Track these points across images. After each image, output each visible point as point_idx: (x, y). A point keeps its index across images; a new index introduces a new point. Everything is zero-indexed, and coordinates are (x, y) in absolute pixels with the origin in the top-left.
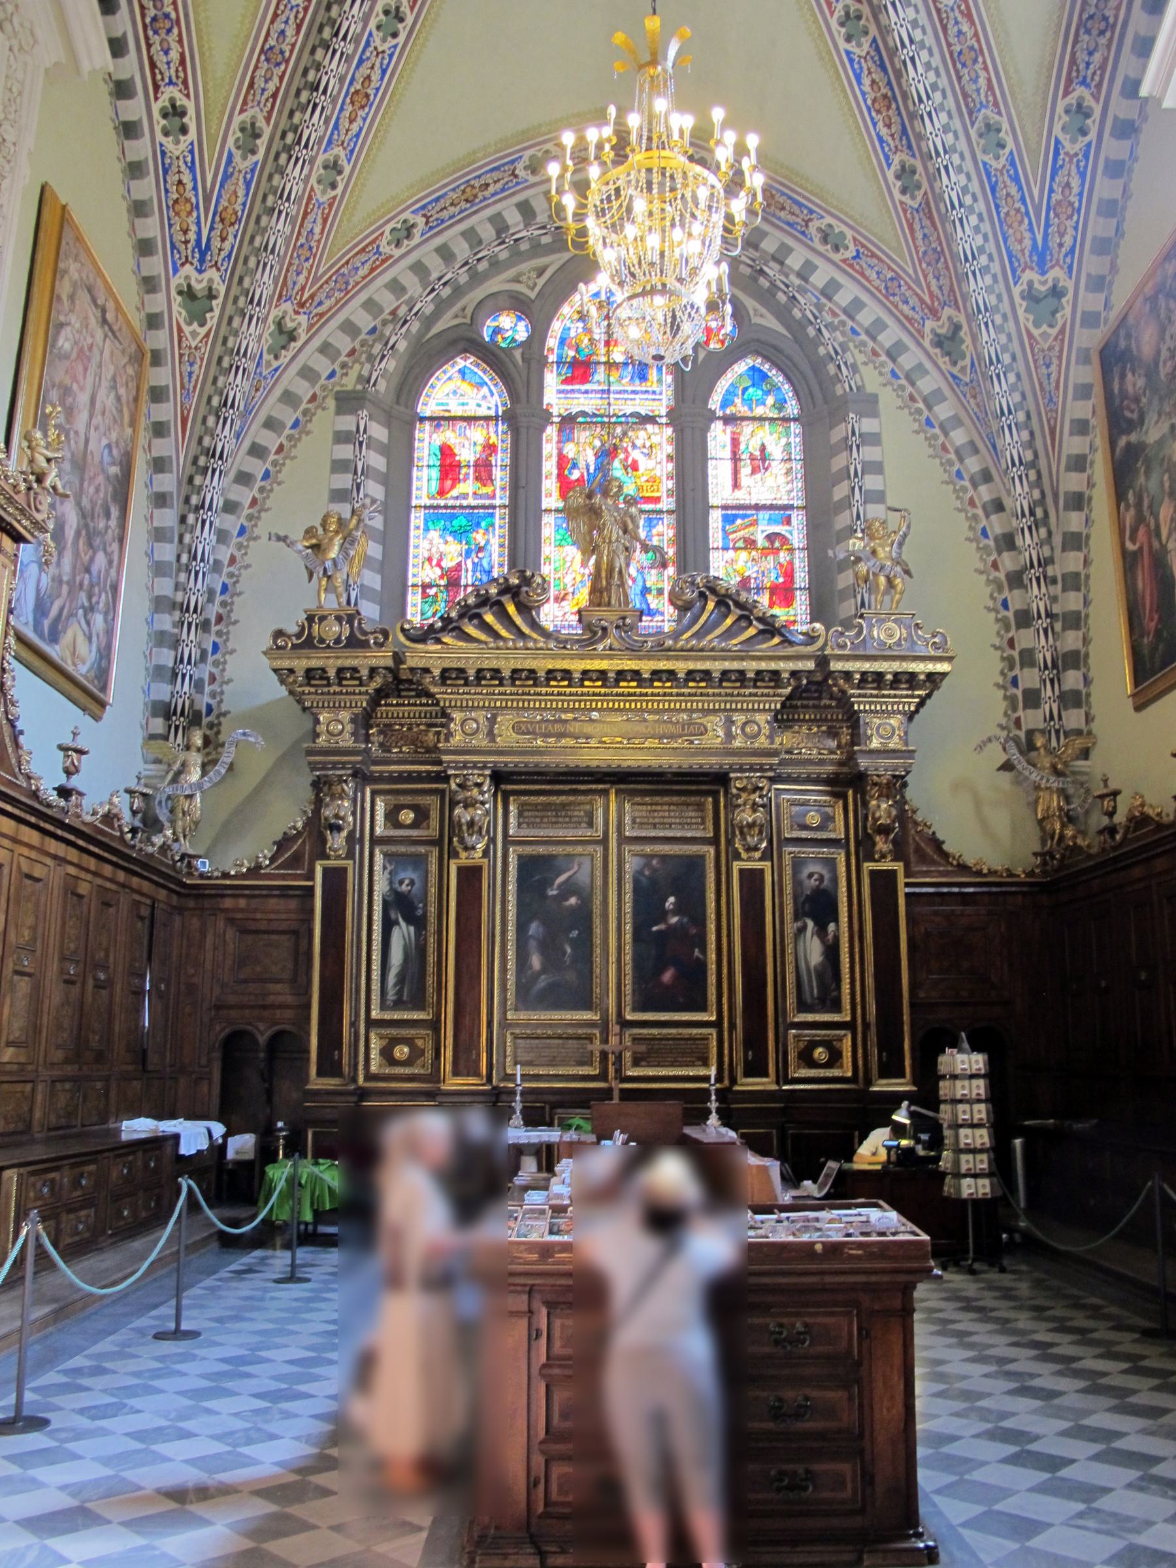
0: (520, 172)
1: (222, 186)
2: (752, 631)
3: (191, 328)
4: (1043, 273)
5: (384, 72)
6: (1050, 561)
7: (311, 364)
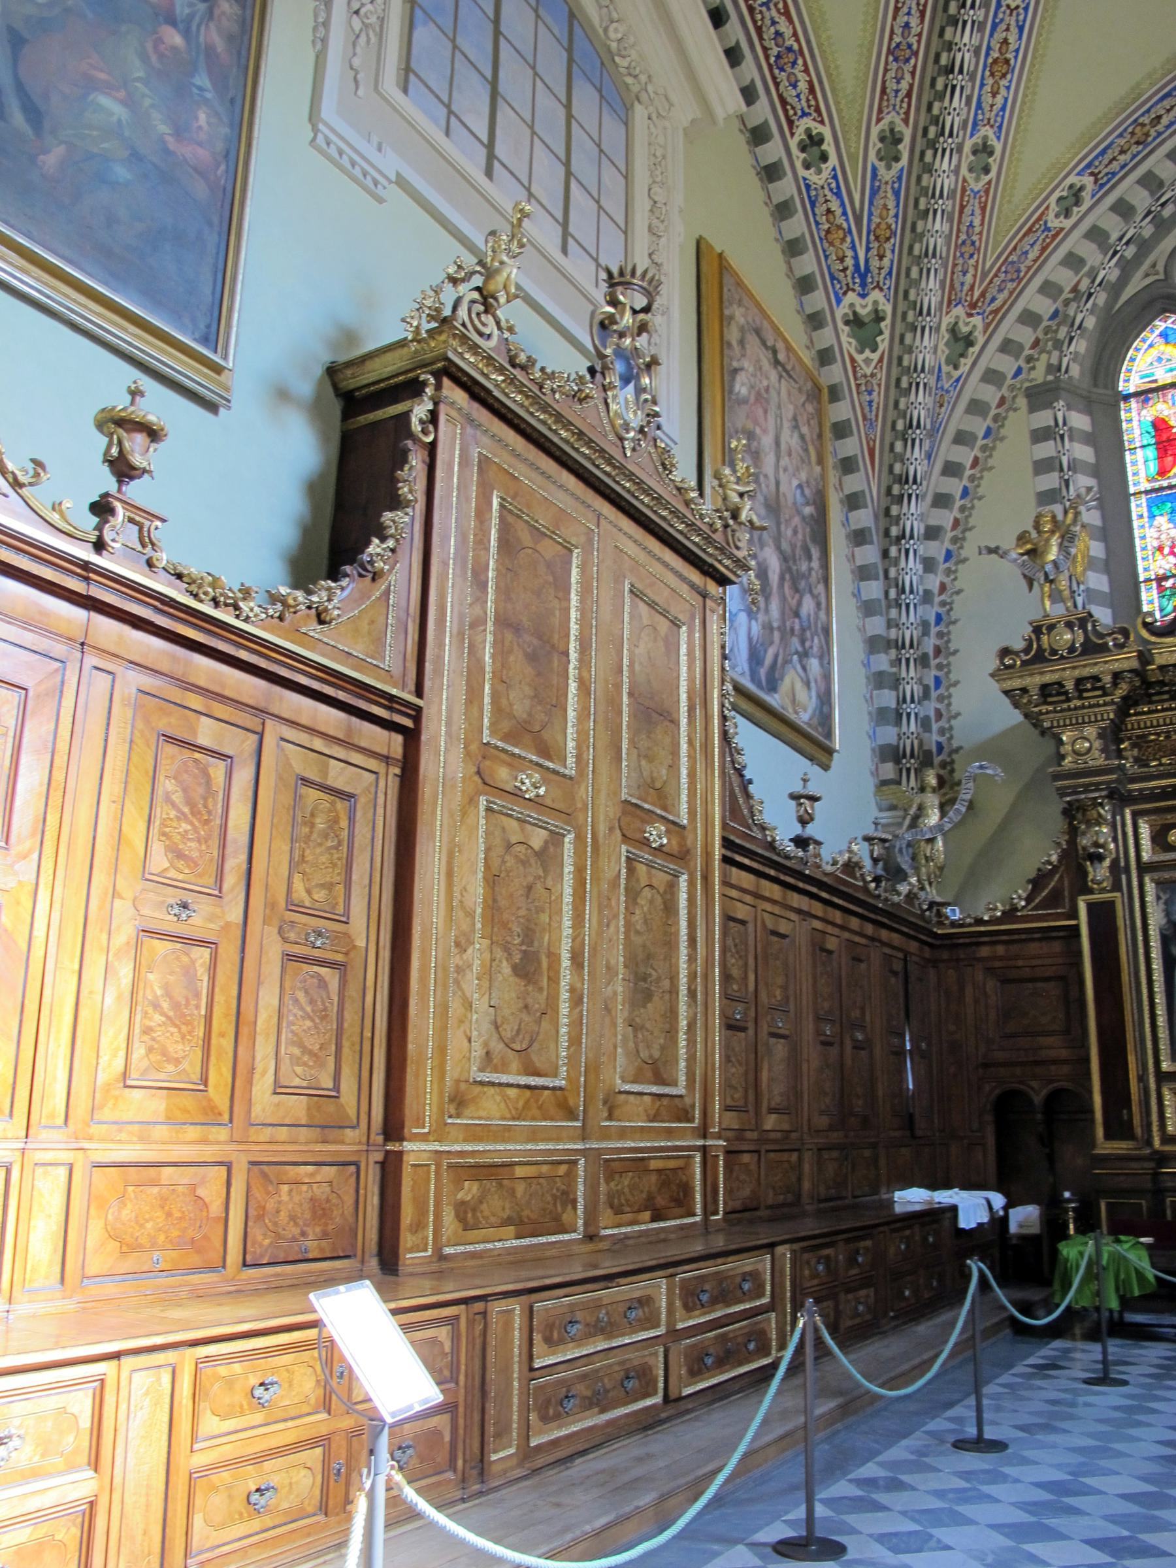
1: (871, 203)
7: (992, 366)
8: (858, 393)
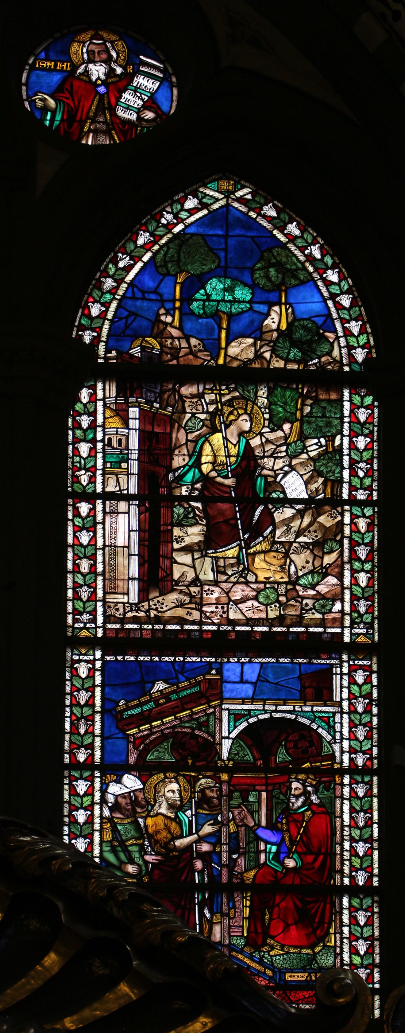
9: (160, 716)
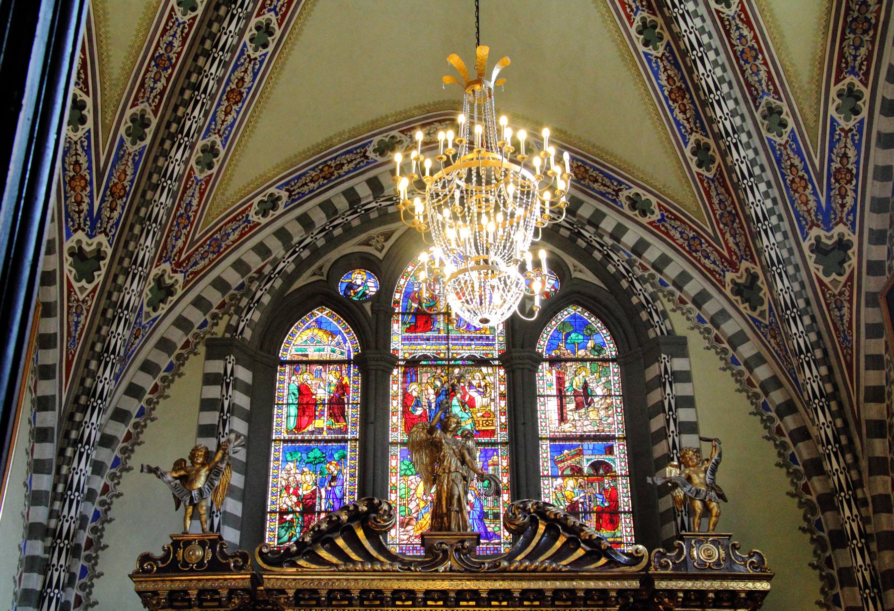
0: (371, 154)
1: (113, 166)
2: (580, 552)
3: (80, 285)
4: (829, 230)
5: (255, 75)
6: (858, 484)
7: (185, 314)
8: (68, 313)
9: (567, 460)
